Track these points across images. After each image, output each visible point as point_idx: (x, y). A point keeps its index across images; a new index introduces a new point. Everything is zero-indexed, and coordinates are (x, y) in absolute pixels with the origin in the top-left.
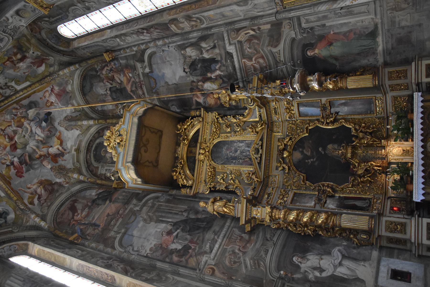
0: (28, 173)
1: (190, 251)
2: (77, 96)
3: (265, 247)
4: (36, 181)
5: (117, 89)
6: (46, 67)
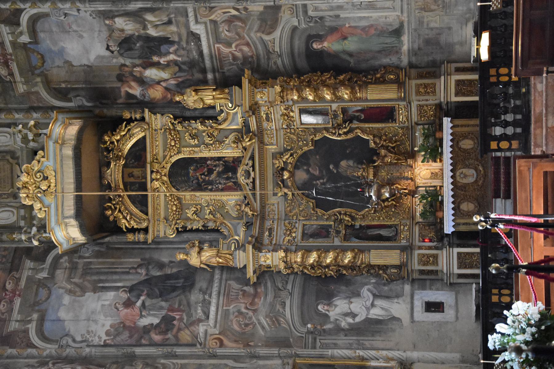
1: (175, 322)
3: (280, 299)
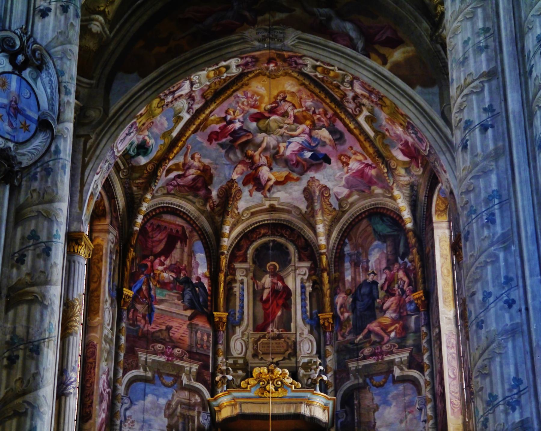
0: (218, 147)
2: (367, 201)
4: (206, 161)
5: (374, 299)
6: (404, 162)
